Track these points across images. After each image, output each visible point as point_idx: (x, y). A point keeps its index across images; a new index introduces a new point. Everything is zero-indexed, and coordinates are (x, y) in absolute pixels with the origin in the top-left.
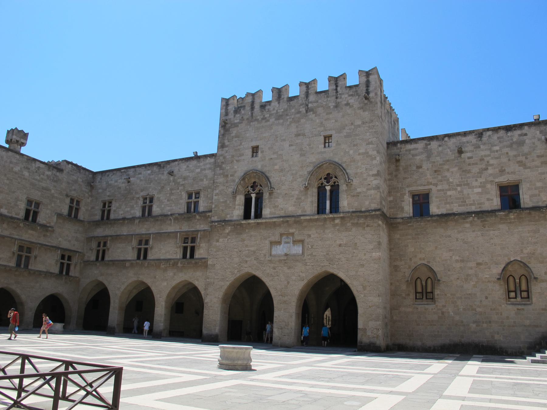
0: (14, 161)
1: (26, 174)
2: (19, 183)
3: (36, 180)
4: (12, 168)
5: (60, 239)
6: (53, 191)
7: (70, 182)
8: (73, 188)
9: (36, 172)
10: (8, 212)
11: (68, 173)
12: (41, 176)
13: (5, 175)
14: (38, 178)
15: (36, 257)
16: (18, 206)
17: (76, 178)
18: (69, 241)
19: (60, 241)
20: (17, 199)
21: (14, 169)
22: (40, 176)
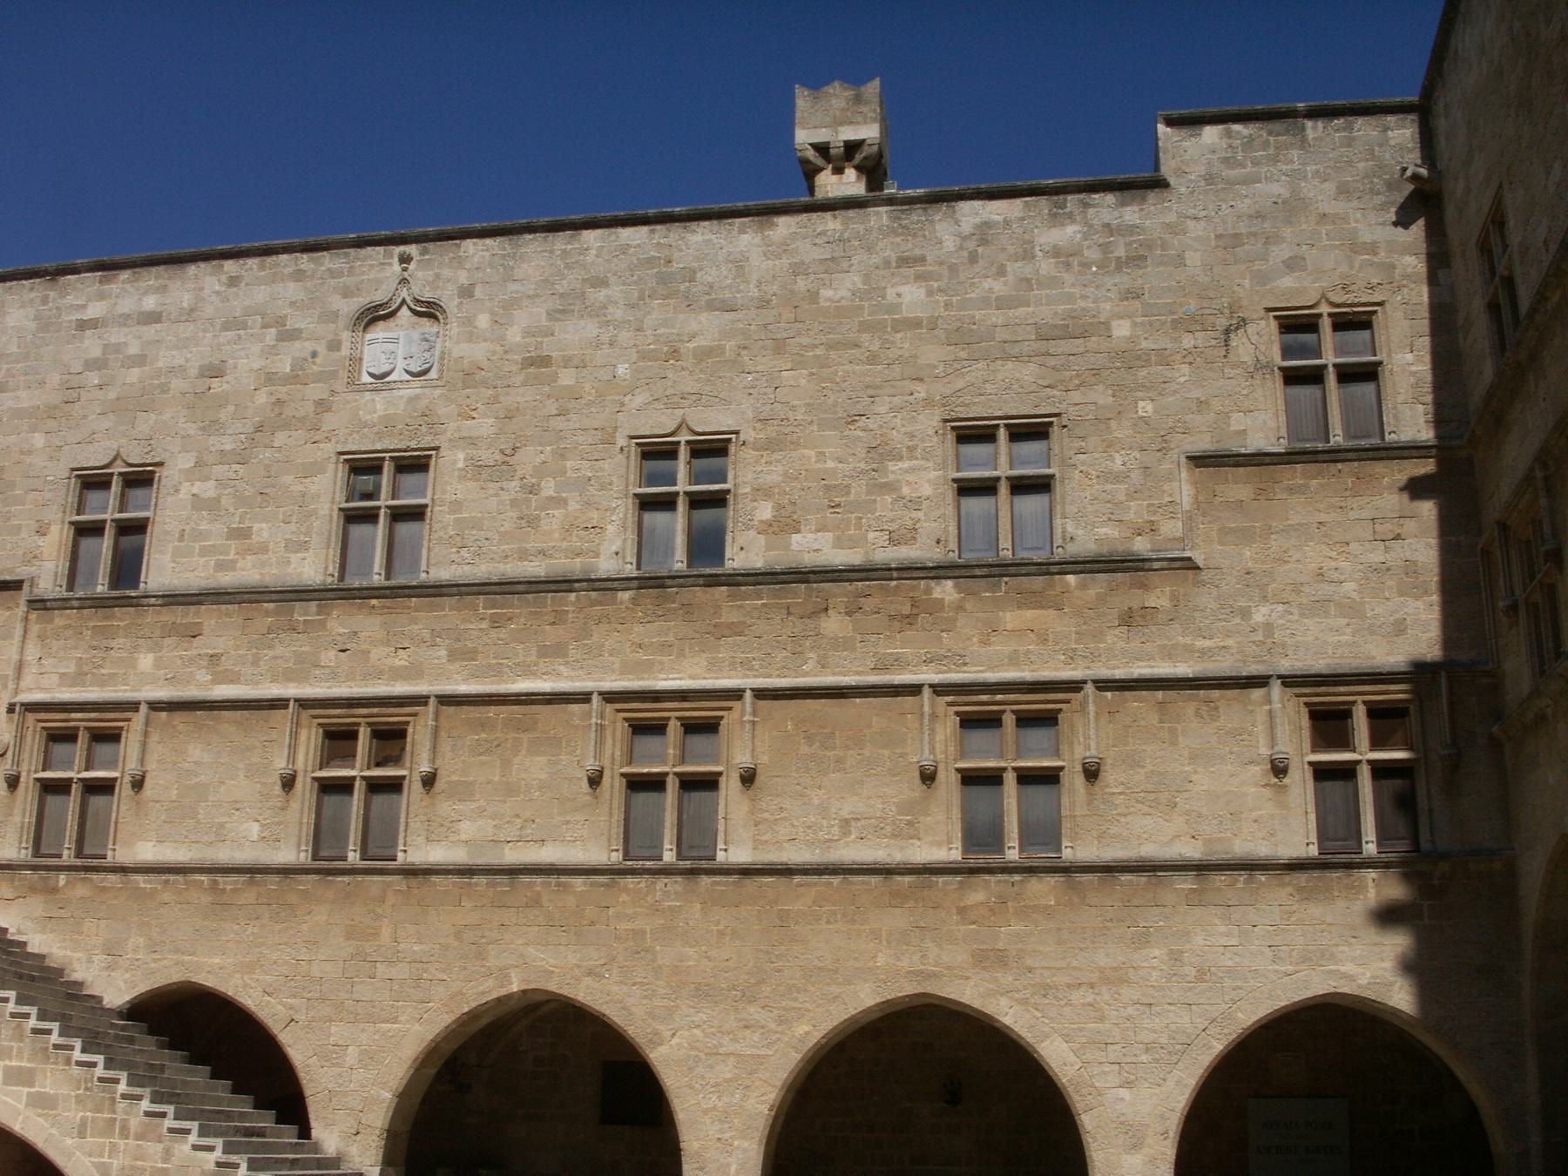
0: (810, 252)
1: (911, 296)
2: (873, 359)
3: (985, 302)
4: (813, 296)
5: (1260, 615)
6: (1122, 329)
7: (1243, 228)
8: (1280, 253)
9: (973, 258)
10: (838, 543)
11: (1209, 179)
12: (1011, 267)
13: (779, 347)
14: (999, 287)
15: (1092, 773)
16: (890, 487)
17: (1278, 189)
18: (1352, 610)
19: (1268, 627)
20: (880, 453)
21: (826, 293)
22: (1002, 272)
